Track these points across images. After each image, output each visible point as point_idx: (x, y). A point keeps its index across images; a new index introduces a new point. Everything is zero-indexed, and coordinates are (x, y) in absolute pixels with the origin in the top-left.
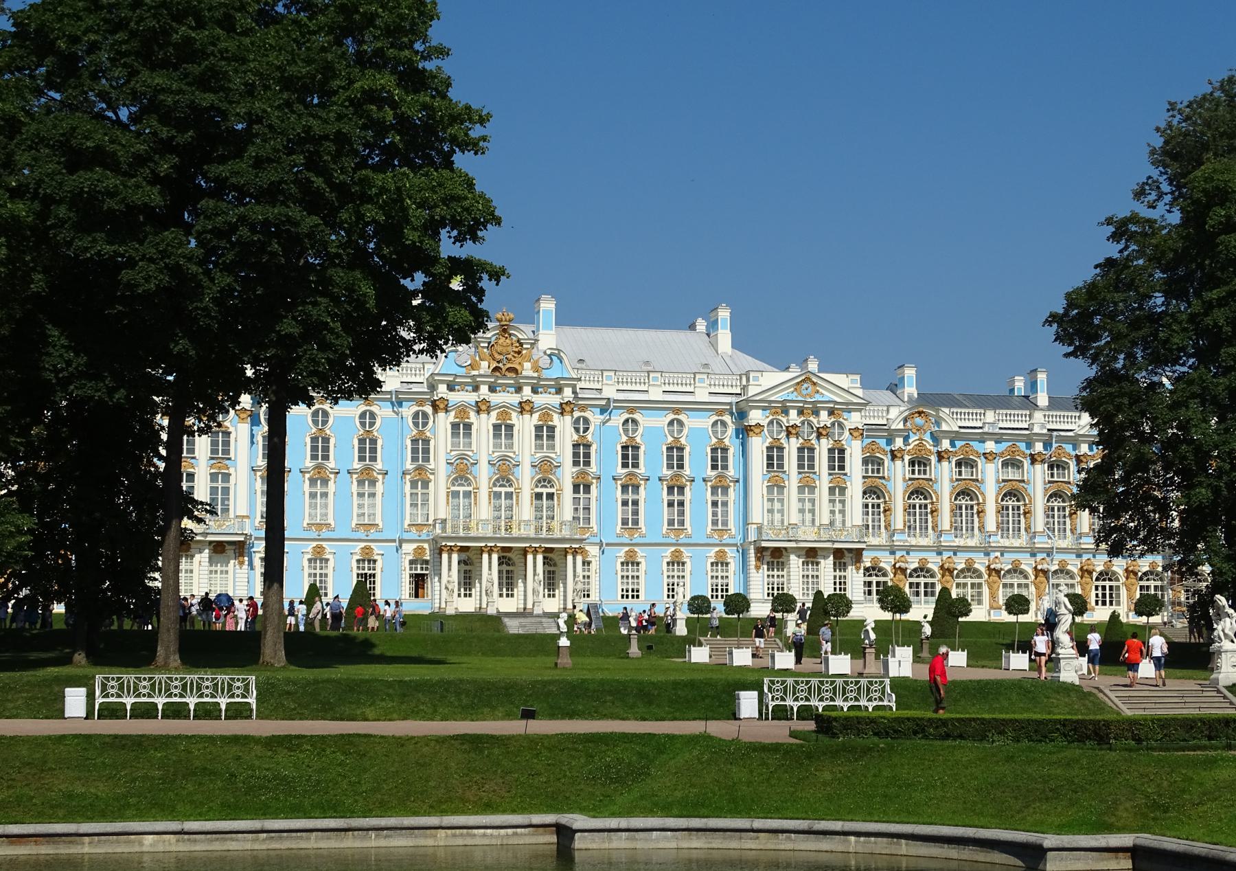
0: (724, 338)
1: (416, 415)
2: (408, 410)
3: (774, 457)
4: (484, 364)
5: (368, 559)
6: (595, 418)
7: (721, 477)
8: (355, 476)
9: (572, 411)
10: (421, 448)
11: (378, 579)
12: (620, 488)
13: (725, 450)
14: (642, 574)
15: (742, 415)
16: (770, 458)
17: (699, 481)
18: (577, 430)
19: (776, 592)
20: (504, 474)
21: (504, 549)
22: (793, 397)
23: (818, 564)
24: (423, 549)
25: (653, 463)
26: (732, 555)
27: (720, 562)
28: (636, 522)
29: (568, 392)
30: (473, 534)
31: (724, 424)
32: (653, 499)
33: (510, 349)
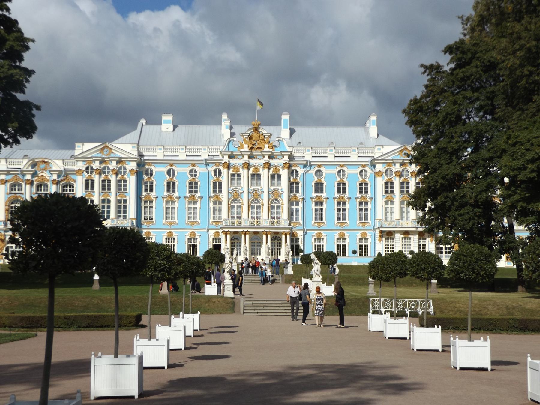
0: (373, 130)
1: (215, 171)
2: (211, 169)
4: (246, 146)
5: (193, 237)
8: (187, 199)
10: (218, 186)
11: (198, 247)
12: (358, 203)
16: (386, 187)
19: (390, 252)
20: (255, 197)
21: (275, 233)
22: (398, 157)
23: (410, 238)
24: (218, 233)
25: (330, 191)
26: (369, 234)
27: (364, 238)
29: (286, 158)
30: (241, 226)
32: (330, 209)
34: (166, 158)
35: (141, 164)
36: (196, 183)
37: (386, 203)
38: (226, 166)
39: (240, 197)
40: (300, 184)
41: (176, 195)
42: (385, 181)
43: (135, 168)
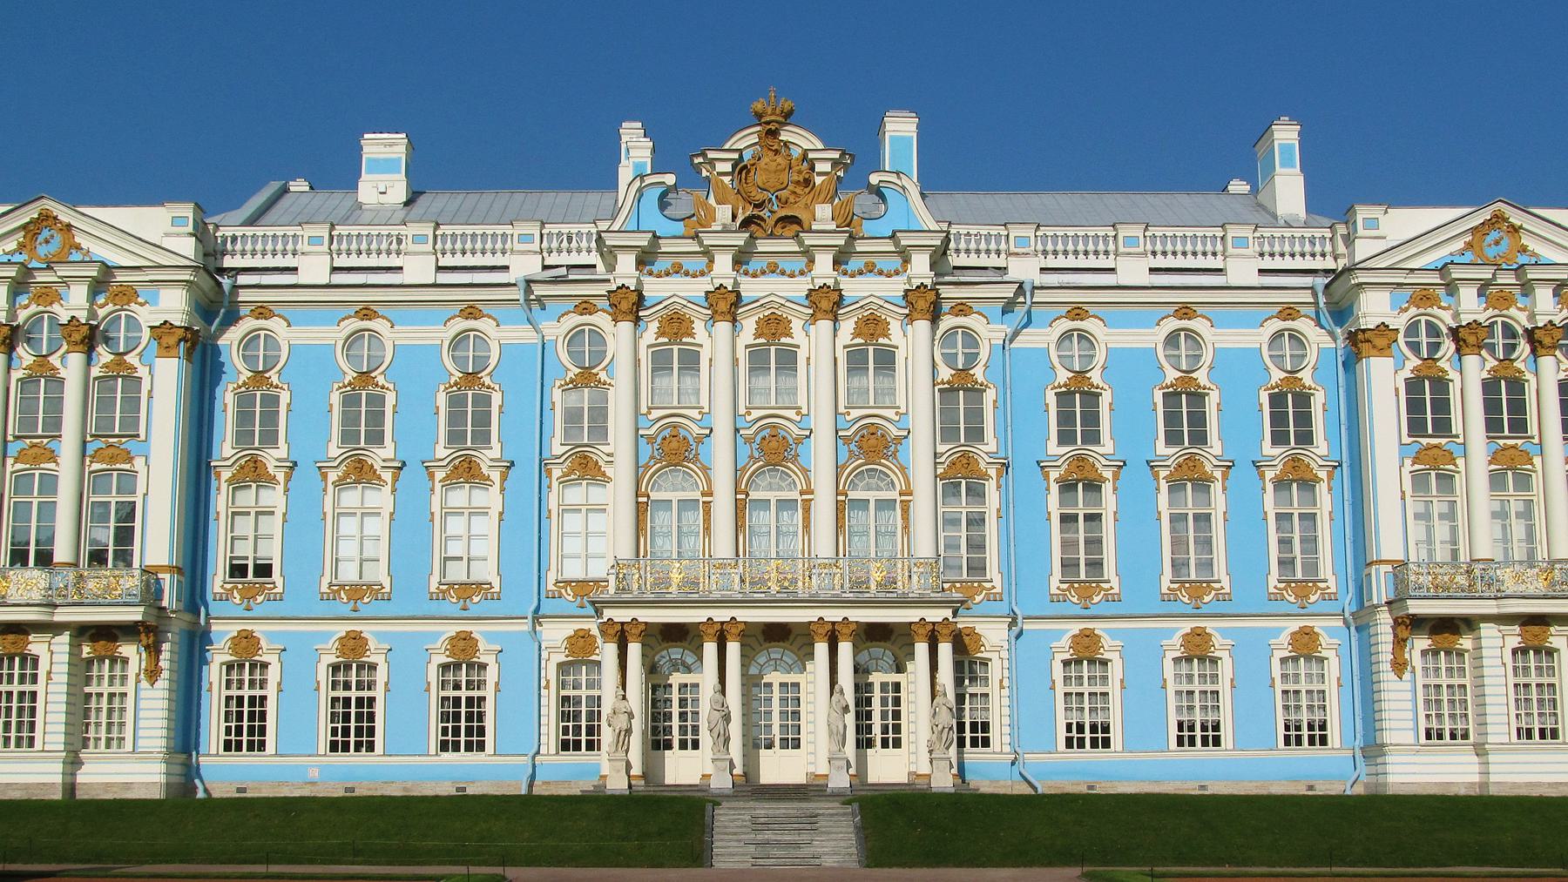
1: (574, 337)
3: (1427, 405)
4: (723, 213)
6: (990, 331)
7: (1295, 463)
9: (935, 318)
13: (1303, 399)
14: (1114, 688)
15: (1340, 311)
16: (1415, 406)
17: (1243, 472)
18: (950, 360)
28: (1096, 565)
29: (920, 267)
31: (1296, 339)
33: (784, 177)
34: (340, 278)
35: (215, 300)
36: (483, 401)
37: (1419, 481)
38: (624, 306)
39: (696, 459)
40: (990, 396)
41: (380, 456)
42: (1407, 373)
43: (178, 320)
